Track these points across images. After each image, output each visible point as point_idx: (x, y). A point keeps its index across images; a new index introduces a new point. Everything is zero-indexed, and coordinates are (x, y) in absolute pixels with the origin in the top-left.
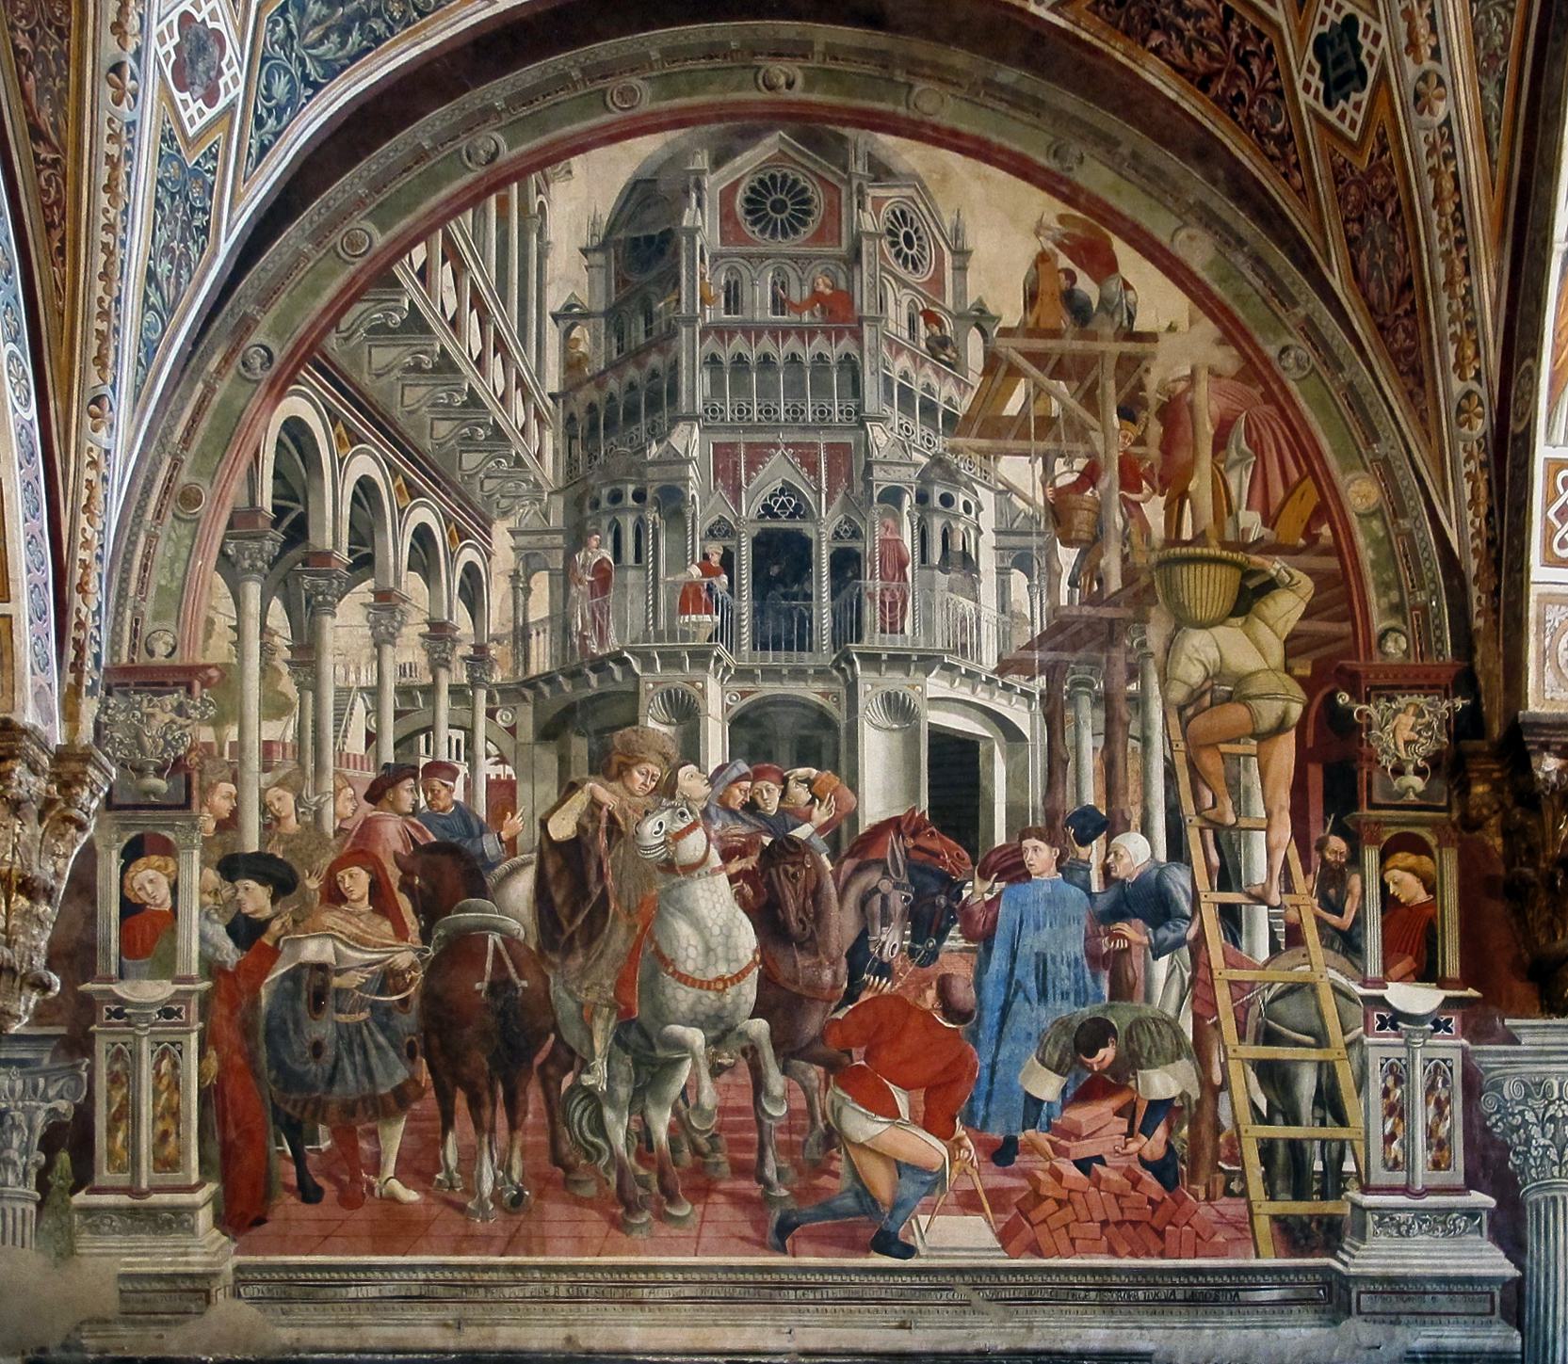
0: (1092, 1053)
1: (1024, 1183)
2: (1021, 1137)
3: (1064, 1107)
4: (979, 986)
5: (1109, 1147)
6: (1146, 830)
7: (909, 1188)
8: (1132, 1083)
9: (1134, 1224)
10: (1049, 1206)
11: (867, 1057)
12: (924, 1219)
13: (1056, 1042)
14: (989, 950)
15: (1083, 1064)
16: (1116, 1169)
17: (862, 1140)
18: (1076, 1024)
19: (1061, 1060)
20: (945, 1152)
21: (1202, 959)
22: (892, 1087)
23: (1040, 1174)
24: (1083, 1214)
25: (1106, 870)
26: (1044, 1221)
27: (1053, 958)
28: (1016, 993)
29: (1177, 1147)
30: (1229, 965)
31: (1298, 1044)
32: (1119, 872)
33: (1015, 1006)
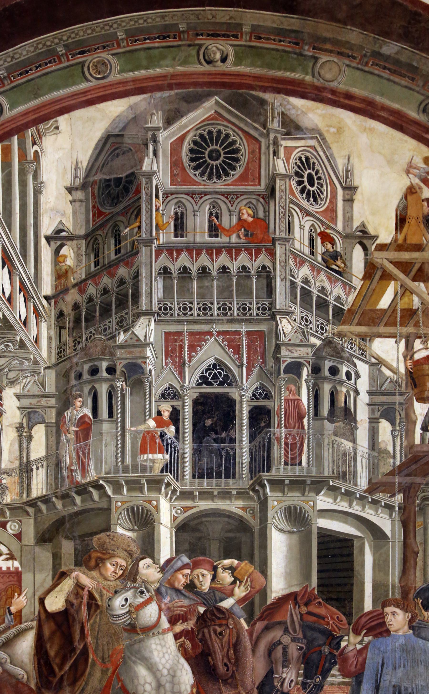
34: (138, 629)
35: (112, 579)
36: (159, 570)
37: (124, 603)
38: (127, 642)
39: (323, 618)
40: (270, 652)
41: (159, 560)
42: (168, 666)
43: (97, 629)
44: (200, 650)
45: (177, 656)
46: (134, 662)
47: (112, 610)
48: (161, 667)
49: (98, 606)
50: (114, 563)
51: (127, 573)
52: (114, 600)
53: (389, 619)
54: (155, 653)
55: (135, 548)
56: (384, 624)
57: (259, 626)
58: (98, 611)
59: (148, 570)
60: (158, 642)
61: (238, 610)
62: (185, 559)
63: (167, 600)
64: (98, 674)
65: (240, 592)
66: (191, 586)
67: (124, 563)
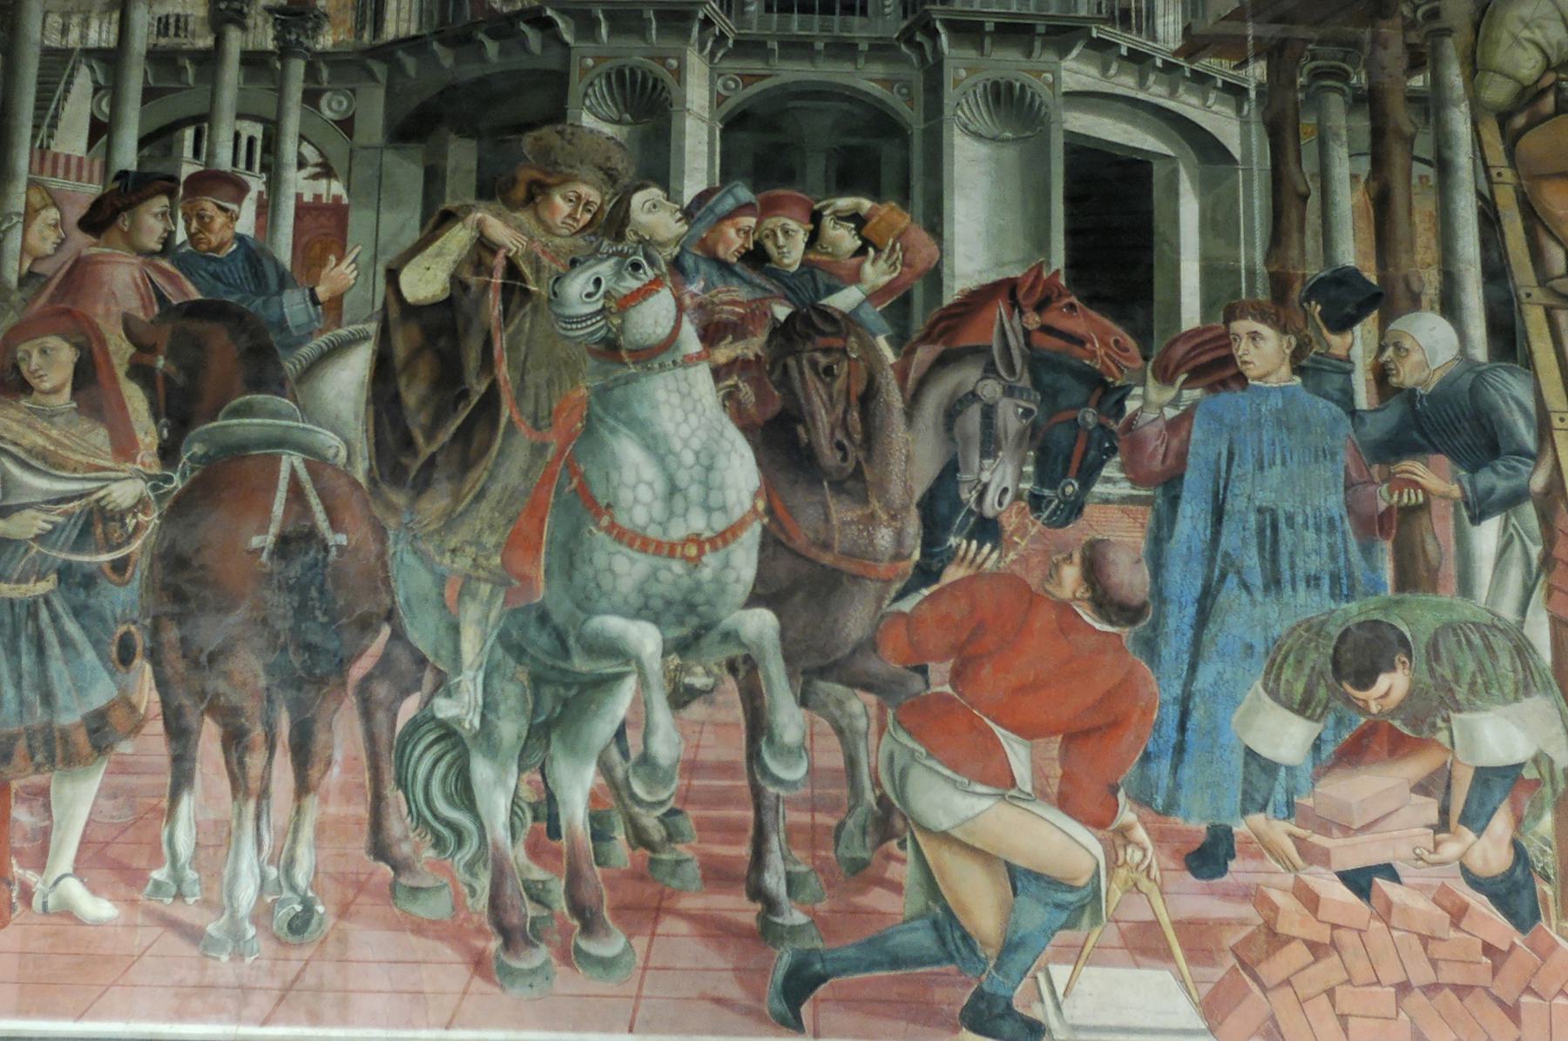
1: (1247, 911)
2: (1240, 828)
3: (1316, 777)
4: (1157, 562)
6: (1450, 306)
7: (1033, 915)
8: (1443, 737)
9: (1461, 990)
10: (1296, 954)
11: (957, 676)
12: (1061, 973)
13: (1299, 662)
14: (1174, 502)
15: (1349, 700)
16: (1421, 888)
18: (1335, 631)
20: (1098, 850)
22: (999, 731)
23: (1277, 897)
24: (1361, 970)
25: (1381, 375)
26: (1287, 982)
27: (1290, 519)
28: (1223, 577)
29: (1532, 852)
32: (1407, 375)
33: (1222, 599)
34: (623, 353)
35: (565, 232)
36: (679, 215)
37: (591, 288)
38: (597, 382)
39: (1081, 342)
40: (952, 413)
41: (681, 193)
42: (696, 443)
43: (523, 348)
44: (774, 408)
45: (719, 420)
46: (613, 431)
47: (560, 304)
48: (677, 445)
49: (526, 293)
50: (572, 196)
51: (603, 218)
52: (567, 281)
53: (1244, 350)
54: (665, 412)
55: (623, 164)
56: (1230, 360)
57: (924, 355)
58: (528, 307)
59: (652, 214)
60: (672, 385)
61: (871, 315)
62: (744, 194)
63: (696, 287)
64: (519, 456)
65: (876, 273)
66: (757, 257)
67: (594, 196)
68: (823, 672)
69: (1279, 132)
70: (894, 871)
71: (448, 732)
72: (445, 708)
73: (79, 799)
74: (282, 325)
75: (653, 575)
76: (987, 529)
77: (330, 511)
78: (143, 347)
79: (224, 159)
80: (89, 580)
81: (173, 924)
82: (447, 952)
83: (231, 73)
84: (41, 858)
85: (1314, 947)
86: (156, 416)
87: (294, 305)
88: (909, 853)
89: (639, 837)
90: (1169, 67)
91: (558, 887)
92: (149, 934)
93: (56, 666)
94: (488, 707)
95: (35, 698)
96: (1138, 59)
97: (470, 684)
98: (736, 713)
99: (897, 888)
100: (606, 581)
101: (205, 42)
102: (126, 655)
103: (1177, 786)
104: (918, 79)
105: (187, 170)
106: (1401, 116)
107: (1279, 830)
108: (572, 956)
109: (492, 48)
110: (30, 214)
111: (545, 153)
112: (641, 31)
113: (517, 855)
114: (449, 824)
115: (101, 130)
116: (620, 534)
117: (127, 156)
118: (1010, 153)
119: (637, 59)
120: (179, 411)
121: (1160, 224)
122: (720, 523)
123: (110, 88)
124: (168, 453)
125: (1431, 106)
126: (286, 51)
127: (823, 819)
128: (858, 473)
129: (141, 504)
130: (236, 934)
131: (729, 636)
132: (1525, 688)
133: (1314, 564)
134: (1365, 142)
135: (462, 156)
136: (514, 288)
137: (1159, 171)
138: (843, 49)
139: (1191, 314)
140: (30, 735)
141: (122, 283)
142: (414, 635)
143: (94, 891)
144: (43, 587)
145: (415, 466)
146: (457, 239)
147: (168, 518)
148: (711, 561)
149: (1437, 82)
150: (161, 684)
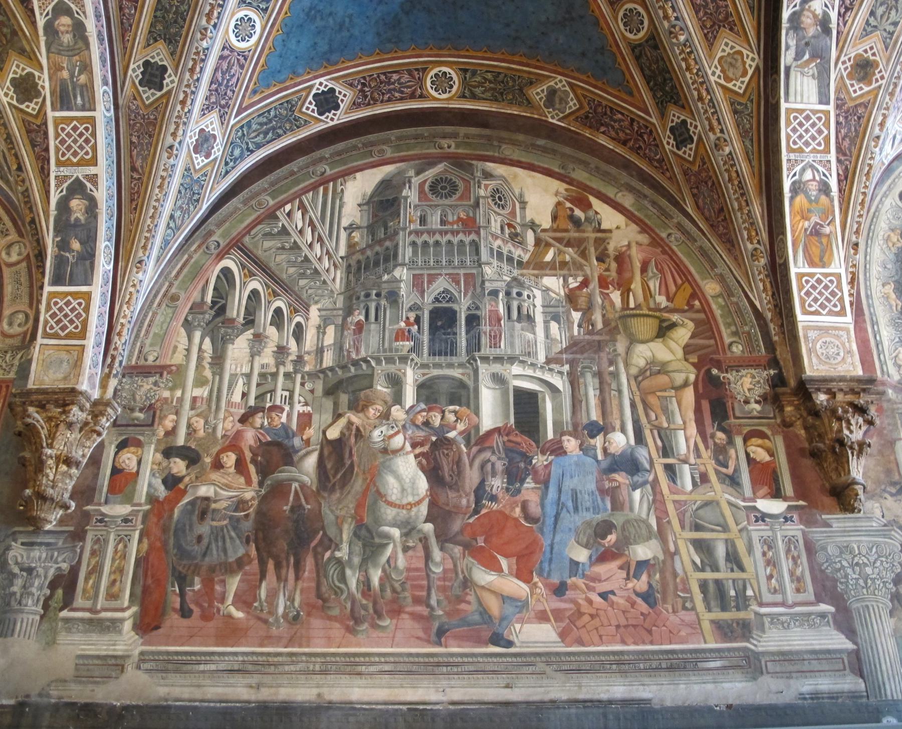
0: (604, 537)
1: (571, 606)
2: (569, 581)
4: (543, 506)
5: (617, 586)
6: (623, 430)
7: (509, 609)
9: (634, 626)
10: (586, 618)
11: (485, 541)
12: (518, 626)
14: (547, 488)
15: (600, 544)
17: (483, 583)
18: (595, 524)
19: (588, 541)
21: (658, 490)
23: (580, 601)
24: (606, 622)
25: (605, 450)
29: (654, 585)
30: (672, 492)
31: (713, 531)
39: (519, 444)
40: (482, 467)
49: (362, 436)
53: (566, 444)
55: (389, 399)
56: (562, 447)
57: (475, 449)
59: (397, 413)
61: (460, 439)
62: (423, 406)
63: (410, 432)
65: (461, 427)
66: (427, 424)
68: (446, 541)
69: (574, 381)
70: (469, 598)
71: (339, 561)
72: (338, 554)
73: (234, 584)
74: (293, 446)
75: (398, 514)
76: (493, 498)
77: (306, 499)
78: (255, 455)
79: (278, 403)
80: (238, 520)
81: (259, 619)
82: (337, 625)
83: (281, 379)
84: (223, 600)
85: (592, 616)
86: (257, 473)
87: (297, 442)
88: (472, 593)
89: (394, 590)
90: (542, 367)
91: (371, 605)
92: (252, 622)
93: (228, 544)
94: (350, 553)
95: (222, 554)
96: (532, 365)
97: (345, 547)
98: (421, 553)
99: (469, 603)
100: (384, 516)
101: (274, 370)
102: (248, 542)
103: (550, 570)
104: (472, 373)
105: (268, 405)
106: (608, 378)
107: (580, 582)
108: (375, 626)
109: (352, 369)
110: (225, 419)
111: (367, 397)
112: (394, 363)
113: (359, 596)
114: (339, 588)
115: (244, 395)
116: (391, 504)
117: (252, 402)
118: (498, 392)
119: (393, 370)
120: (264, 472)
121: (541, 411)
122: (417, 499)
123: (248, 384)
124: (261, 484)
125: (615, 375)
126: (296, 371)
127: (447, 583)
128: (456, 483)
129: (253, 499)
130: (277, 620)
131: (420, 531)
132: (649, 538)
133: (588, 504)
134: (597, 386)
135: (344, 398)
136: (359, 434)
137: (540, 396)
138: (450, 366)
139: (550, 435)
140: (220, 564)
141: (250, 437)
142: (328, 533)
143: (237, 609)
144: (225, 522)
145: (330, 485)
146: (342, 422)
147: (260, 503)
148: (414, 510)
149: (617, 368)
150: (257, 549)
